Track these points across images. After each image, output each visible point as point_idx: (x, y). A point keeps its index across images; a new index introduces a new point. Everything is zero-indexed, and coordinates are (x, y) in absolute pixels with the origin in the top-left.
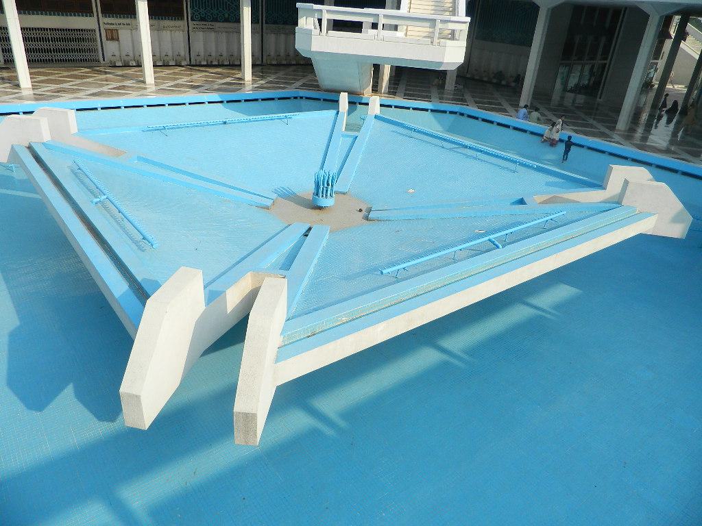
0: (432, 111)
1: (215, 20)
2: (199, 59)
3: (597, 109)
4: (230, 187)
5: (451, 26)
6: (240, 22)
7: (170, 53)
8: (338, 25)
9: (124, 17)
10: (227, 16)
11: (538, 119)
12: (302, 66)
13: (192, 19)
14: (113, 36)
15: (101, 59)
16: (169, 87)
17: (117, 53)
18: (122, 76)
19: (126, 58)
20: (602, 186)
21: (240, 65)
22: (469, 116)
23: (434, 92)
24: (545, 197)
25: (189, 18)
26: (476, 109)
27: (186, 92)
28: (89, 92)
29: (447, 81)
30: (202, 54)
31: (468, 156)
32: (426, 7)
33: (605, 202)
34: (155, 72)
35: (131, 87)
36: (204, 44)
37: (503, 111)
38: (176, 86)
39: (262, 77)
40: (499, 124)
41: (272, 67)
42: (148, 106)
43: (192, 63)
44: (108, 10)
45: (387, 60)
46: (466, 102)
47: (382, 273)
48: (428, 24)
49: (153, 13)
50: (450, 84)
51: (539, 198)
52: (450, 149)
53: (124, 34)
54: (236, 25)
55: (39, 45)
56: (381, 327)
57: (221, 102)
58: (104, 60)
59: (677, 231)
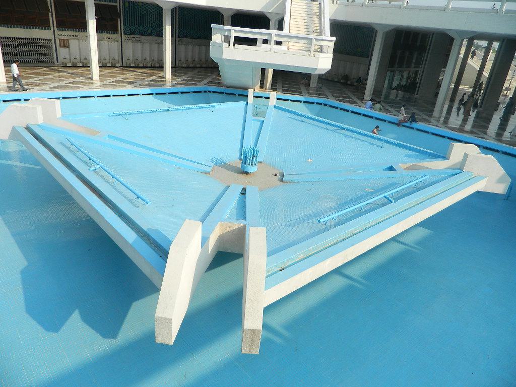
0: (304, 102)
1: (141, 34)
4: (180, 158)
5: (322, 43)
7: (107, 58)
8: (239, 41)
11: (380, 109)
12: (211, 68)
14: (65, 44)
17: (68, 57)
18: (71, 73)
19: (74, 61)
20: (444, 156)
21: (163, 67)
23: (303, 89)
24: (408, 165)
25: (123, 32)
27: (125, 86)
28: (51, 86)
29: (311, 82)
30: (131, 58)
31: (346, 136)
32: (300, 29)
33: (448, 168)
34: (100, 71)
35: (82, 82)
36: (133, 52)
38: (117, 82)
39: (178, 76)
40: (353, 112)
43: (124, 65)
44: (61, 25)
45: (271, 65)
46: (326, 96)
47: (319, 222)
48: (306, 42)
49: (100, 28)
50: (314, 83)
52: (333, 130)
53: (73, 43)
55: (13, 50)
56: (328, 261)
58: (58, 62)
59: (501, 189)
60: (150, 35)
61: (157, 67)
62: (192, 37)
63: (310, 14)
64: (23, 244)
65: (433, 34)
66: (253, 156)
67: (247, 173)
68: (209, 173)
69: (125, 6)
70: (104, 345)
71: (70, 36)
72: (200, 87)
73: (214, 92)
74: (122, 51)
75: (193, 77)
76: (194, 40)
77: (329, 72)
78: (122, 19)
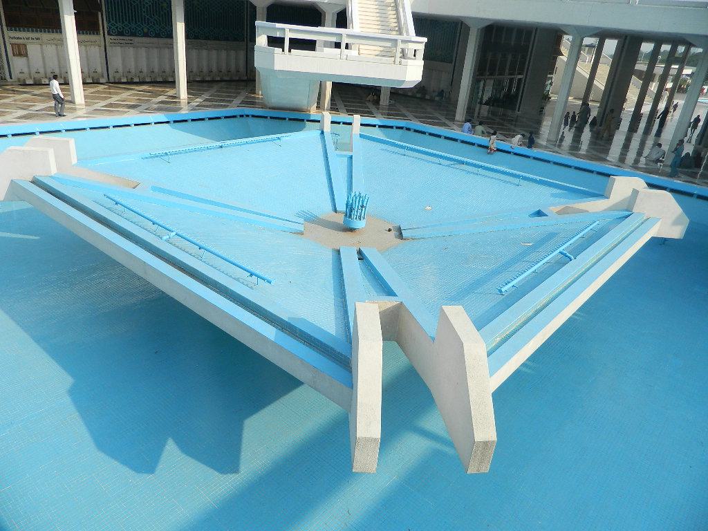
0: (380, 126)
1: (134, 35)
2: (118, 76)
3: (516, 121)
6: (172, 37)
8: (297, 44)
9: (33, 31)
10: (145, 30)
11: (483, 132)
13: (109, 34)
14: (21, 51)
15: (9, 79)
16: (103, 106)
17: (26, 70)
19: (37, 76)
20: (602, 194)
21: (174, 82)
22: (416, 131)
23: (373, 109)
24: (559, 208)
26: (419, 123)
30: (121, 70)
32: (371, 26)
37: (444, 125)
38: (111, 105)
40: (446, 138)
42: (91, 128)
43: (111, 81)
45: (329, 76)
47: (500, 291)
48: (389, 44)
50: (385, 99)
51: (555, 209)
52: (448, 166)
53: (33, 49)
54: (169, 40)
56: (531, 343)
57: (168, 122)
60: (146, 35)
62: (207, 38)
64: (59, 353)
65: (536, 30)
66: (362, 206)
67: (352, 230)
68: (302, 233)
70: (219, 486)
71: (28, 39)
72: (232, 110)
73: (253, 116)
74: (106, 57)
76: (209, 42)
78: (104, 13)
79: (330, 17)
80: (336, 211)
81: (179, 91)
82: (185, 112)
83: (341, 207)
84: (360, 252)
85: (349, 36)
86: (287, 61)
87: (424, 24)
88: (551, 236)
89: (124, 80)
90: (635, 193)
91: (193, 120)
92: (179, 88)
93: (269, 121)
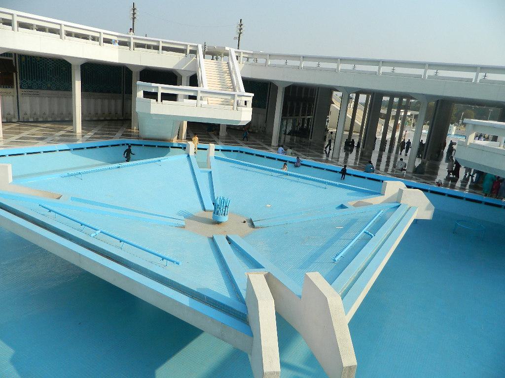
0: (222, 150)
2: (26, 117)
4: (151, 214)
8: (167, 97)
11: (292, 154)
13: (21, 87)
20: (380, 193)
23: (216, 139)
24: (354, 202)
30: (29, 113)
39: (89, 131)
41: (92, 123)
45: (184, 118)
48: (229, 97)
50: (223, 132)
60: (49, 89)
61: (58, 121)
63: (221, 73)
66: (226, 206)
69: (21, 61)
74: (18, 105)
75: (105, 131)
76: (96, 94)
77: (250, 124)
78: (18, 73)
79: (185, 80)
80: (204, 210)
81: (76, 127)
82: (79, 143)
83: (210, 206)
84: (228, 238)
85: (202, 92)
86: (158, 107)
87: (250, 84)
88: (354, 221)
89: (31, 120)
90: (401, 191)
91: (87, 148)
92: (76, 124)
93: (143, 148)
